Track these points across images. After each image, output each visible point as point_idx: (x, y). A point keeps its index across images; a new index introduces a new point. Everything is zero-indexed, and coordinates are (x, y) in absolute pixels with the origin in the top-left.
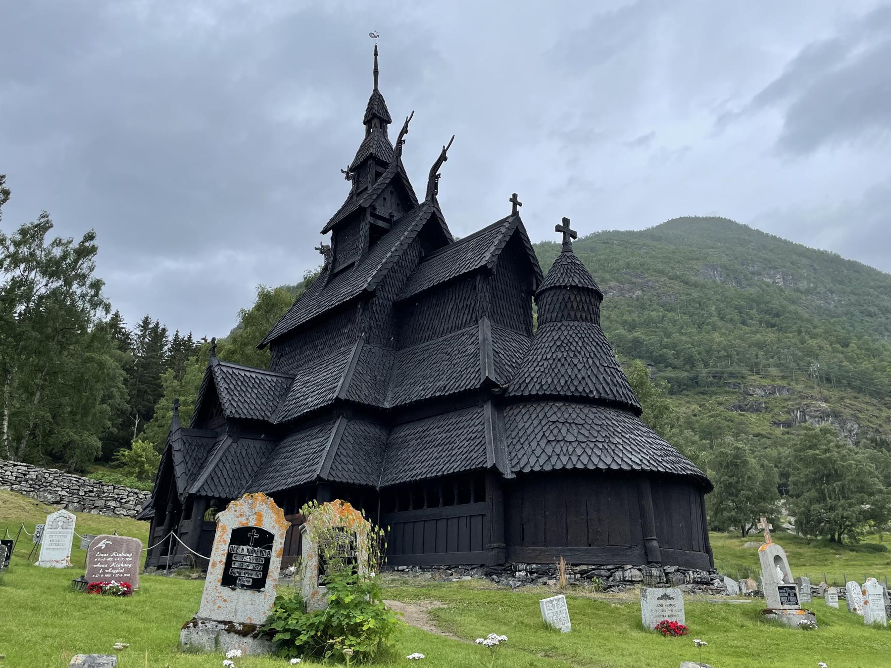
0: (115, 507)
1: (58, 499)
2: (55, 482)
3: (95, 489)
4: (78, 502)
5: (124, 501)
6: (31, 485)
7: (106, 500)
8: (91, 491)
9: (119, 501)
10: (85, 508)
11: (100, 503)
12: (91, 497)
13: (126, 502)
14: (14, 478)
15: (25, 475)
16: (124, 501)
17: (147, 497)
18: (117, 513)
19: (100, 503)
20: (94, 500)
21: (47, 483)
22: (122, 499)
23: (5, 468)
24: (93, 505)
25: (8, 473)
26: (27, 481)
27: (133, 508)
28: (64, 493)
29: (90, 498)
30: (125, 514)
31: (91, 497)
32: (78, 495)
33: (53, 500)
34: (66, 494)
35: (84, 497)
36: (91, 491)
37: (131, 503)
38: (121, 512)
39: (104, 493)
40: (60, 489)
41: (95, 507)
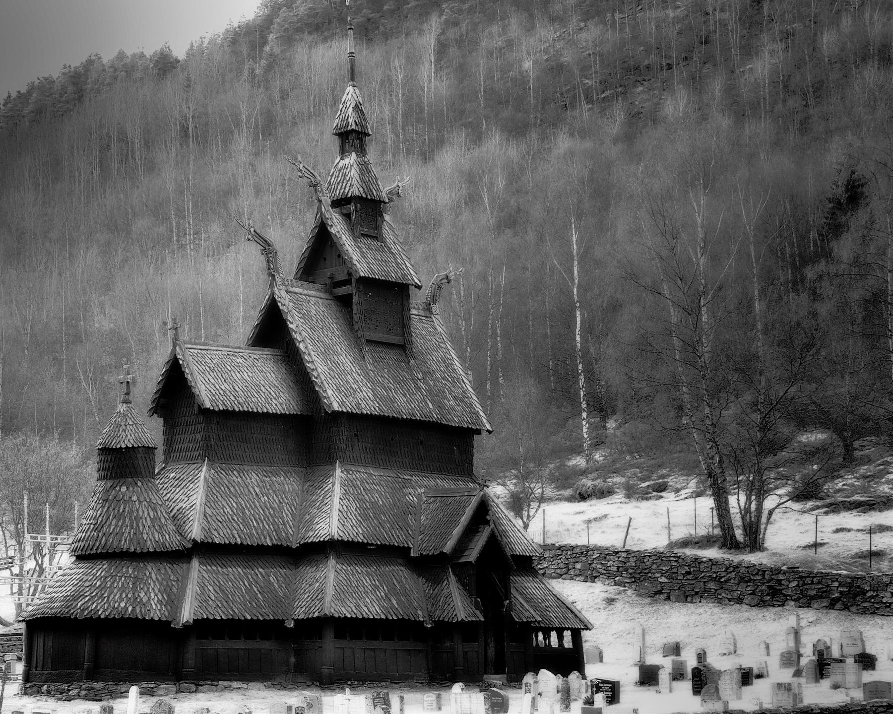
0: (716, 590)
1: (659, 588)
2: (654, 566)
3: (692, 569)
4: (679, 589)
5: (723, 580)
6: (630, 574)
7: (704, 582)
8: (688, 573)
9: (719, 581)
10: (687, 596)
11: (699, 587)
12: (689, 580)
13: (726, 581)
14: (615, 569)
15: (625, 563)
16: (723, 580)
17: (750, 570)
18: (720, 597)
19: (699, 587)
20: (693, 584)
21: (646, 569)
22: (721, 578)
23: (608, 557)
24: (693, 590)
25: (611, 563)
26: (626, 570)
27: (735, 588)
28: (663, 580)
29: (689, 582)
30: (729, 597)
31: (689, 580)
32: (677, 579)
33: (655, 589)
34: (666, 580)
35: (683, 581)
36: (688, 573)
37: (732, 581)
38: (723, 595)
39: (703, 572)
40: (658, 575)
41: (697, 593)
